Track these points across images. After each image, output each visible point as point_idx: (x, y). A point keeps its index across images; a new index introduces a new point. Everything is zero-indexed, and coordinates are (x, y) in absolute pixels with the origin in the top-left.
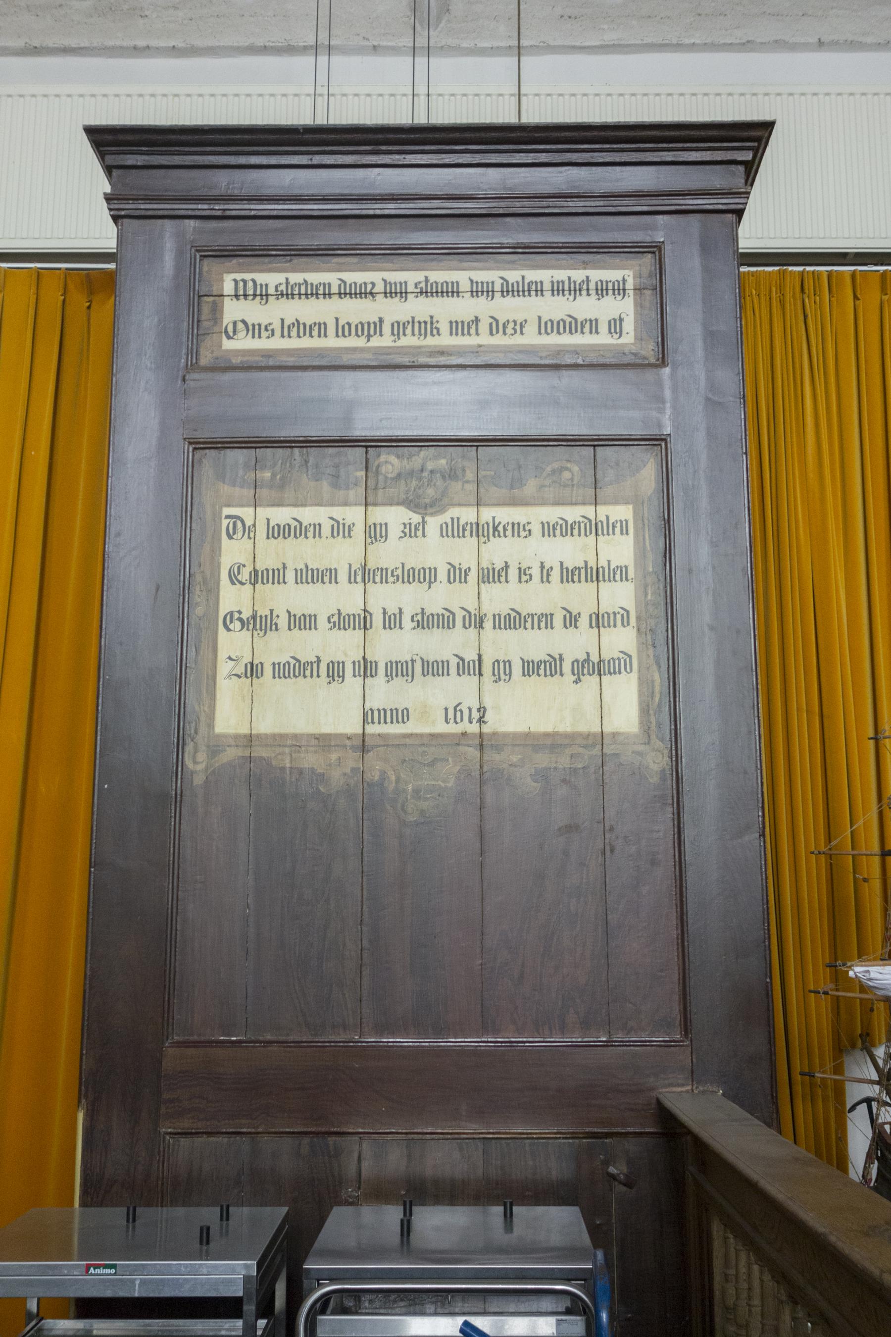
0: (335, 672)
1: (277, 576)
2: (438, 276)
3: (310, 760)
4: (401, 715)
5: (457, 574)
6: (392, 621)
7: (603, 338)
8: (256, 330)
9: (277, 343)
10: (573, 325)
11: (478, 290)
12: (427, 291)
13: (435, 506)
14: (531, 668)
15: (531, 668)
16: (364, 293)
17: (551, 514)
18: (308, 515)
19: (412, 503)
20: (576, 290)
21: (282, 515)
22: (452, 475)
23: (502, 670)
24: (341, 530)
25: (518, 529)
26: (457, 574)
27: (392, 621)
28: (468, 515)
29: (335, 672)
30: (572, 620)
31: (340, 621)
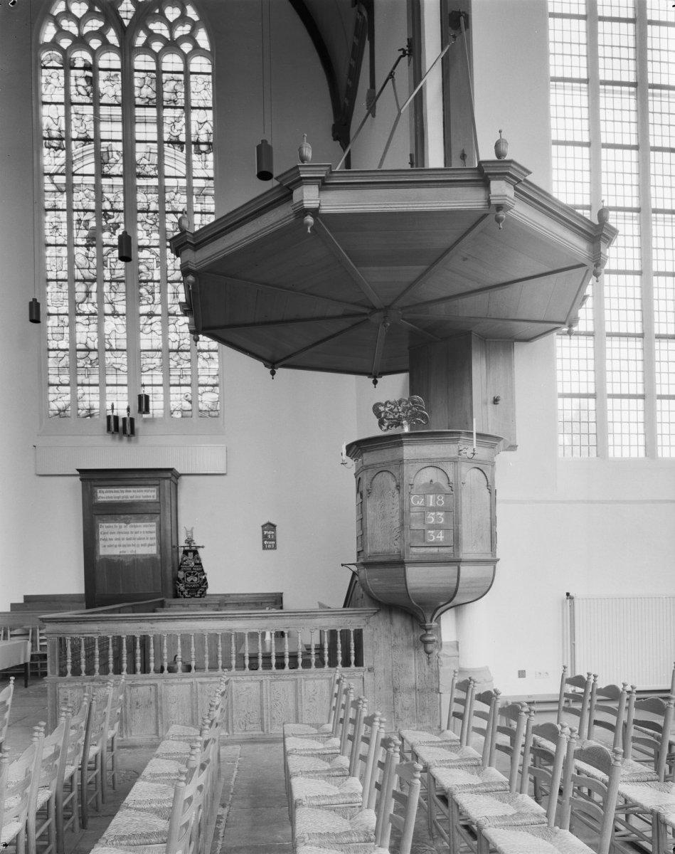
0: (116, 546)
1: (107, 533)
2: (128, 489)
3: (112, 558)
4: (125, 552)
5: (132, 533)
6: (123, 539)
7: (151, 498)
8: (102, 498)
9: (106, 500)
10: (148, 497)
11: (134, 491)
12: (127, 491)
13: (128, 523)
14: (142, 545)
15: (142, 545)
16: (118, 492)
17: (144, 524)
18: (111, 524)
19: (125, 523)
20: (148, 491)
21: (107, 525)
22: (131, 518)
23: (138, 546)
24: (116, 527)
25: (140, 526)
26: (132, 533)
27: (123, 539)
28: (133, 524)
29: (116, 546)
30: (147, 539)
31: (116, 539)
